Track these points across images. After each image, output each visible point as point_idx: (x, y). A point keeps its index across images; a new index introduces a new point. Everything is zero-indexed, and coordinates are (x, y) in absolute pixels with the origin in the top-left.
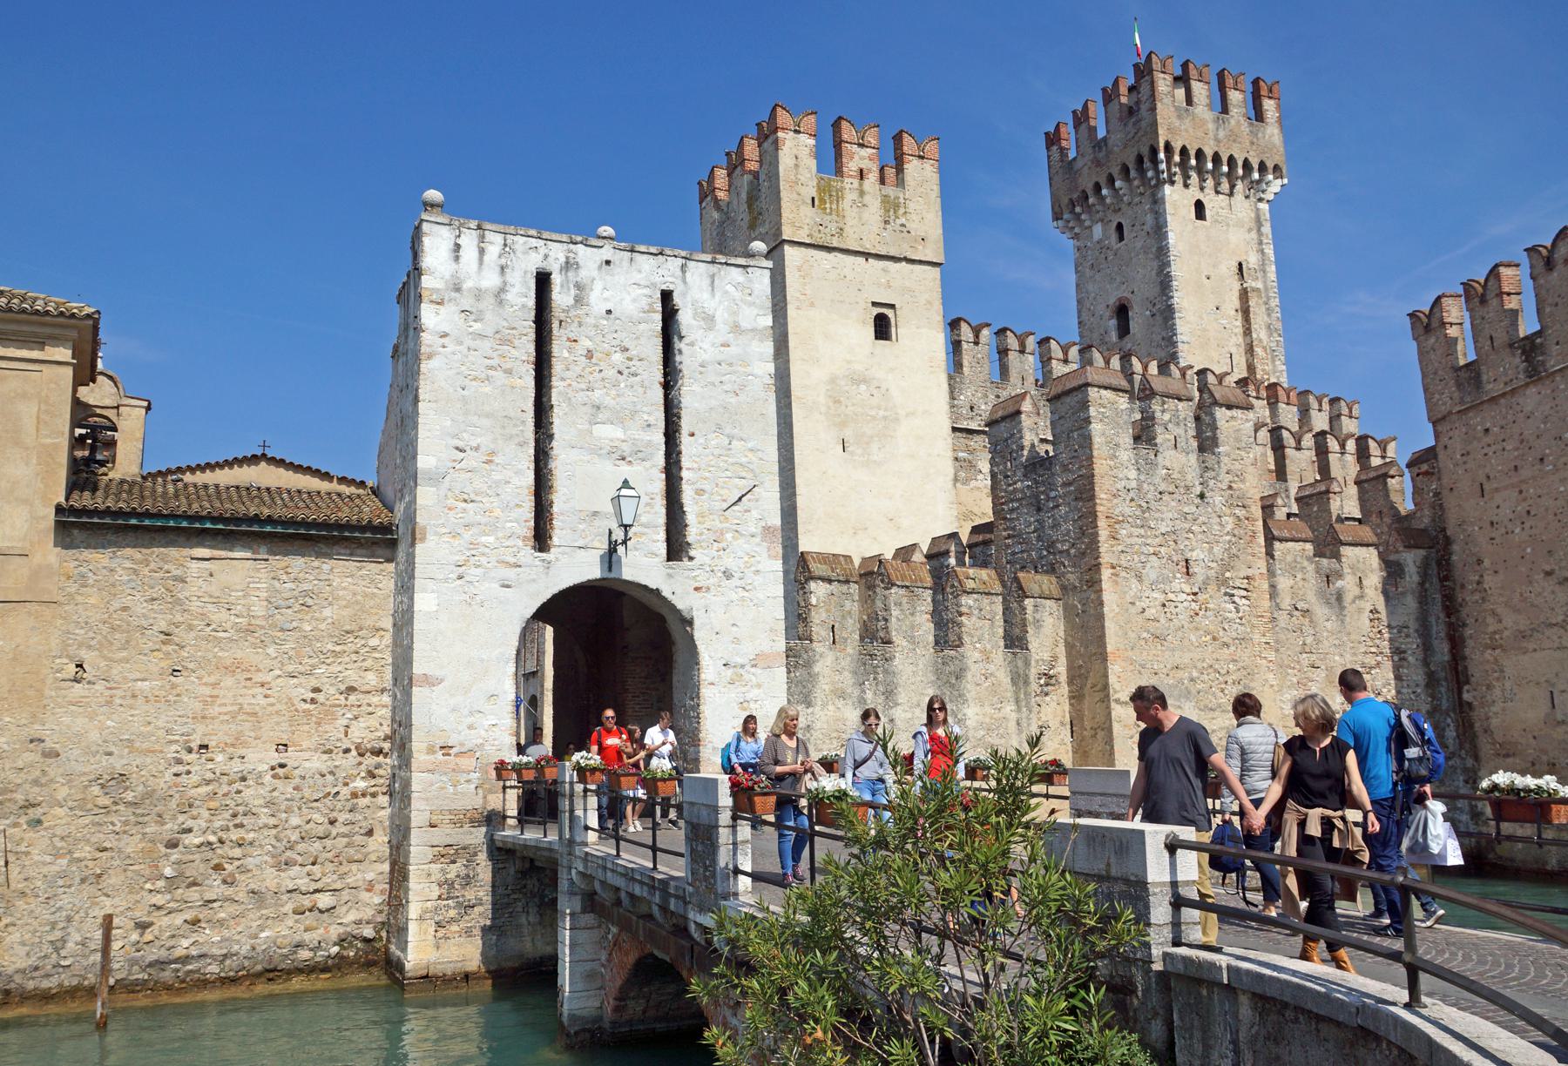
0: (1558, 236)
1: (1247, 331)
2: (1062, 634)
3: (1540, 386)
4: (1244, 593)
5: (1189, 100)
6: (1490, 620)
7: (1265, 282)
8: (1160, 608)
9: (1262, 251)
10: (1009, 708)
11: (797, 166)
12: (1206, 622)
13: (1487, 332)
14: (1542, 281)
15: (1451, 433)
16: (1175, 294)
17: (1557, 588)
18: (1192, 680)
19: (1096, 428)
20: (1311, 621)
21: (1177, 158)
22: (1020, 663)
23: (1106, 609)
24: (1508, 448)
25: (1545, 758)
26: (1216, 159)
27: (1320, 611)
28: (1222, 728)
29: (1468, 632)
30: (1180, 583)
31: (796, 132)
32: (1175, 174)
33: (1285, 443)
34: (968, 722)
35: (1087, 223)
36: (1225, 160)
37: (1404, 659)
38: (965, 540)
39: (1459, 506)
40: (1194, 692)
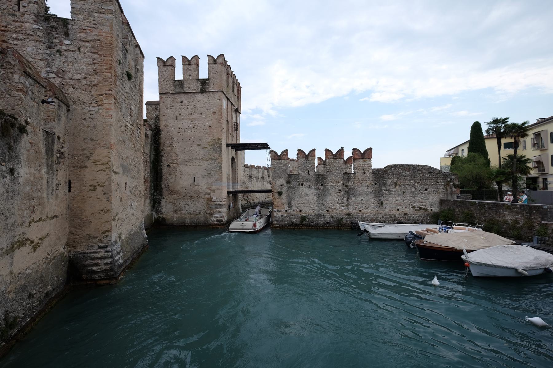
0: (220, 55)
6: (174, 155)
13: (189, 73)
15: (167, 99)
17: (201, 150)
25: (189, 195)
29: (164, 158)
34: (21, 180)
37: (147, 164)
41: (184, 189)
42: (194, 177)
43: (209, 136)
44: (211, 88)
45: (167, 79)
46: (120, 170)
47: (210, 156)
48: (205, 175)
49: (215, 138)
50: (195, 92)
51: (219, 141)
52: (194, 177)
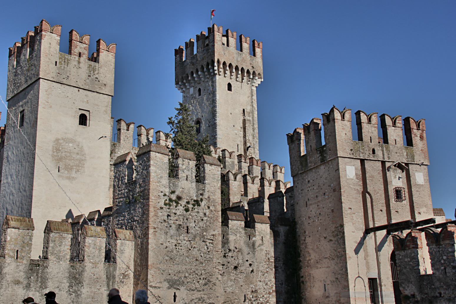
1: (245, 136)
2: (133, 256)
3: (325, 166)
4: (211, 241)
5: (228, 45)
6: (307, 255)
7: (253, 118)
8: (174, 247)
9: (253, 106)
10: (103, 289)
11: (50, 47)
12: (195, 252)
14: (326, 127)
15: (298, 181)
16: (217, 119)
18: (185, 277)
19: (152, 169)
20: (242, 254)
21: (221, 66)
22: (111, 269)
23: (150, 246)
24: (315, 188)
26: (237, 68)
27: (246, 250)
28: (197, 298)
30: (184, 237)
31: (51, 32)
32: (221, 72)
33: (248, 181)
34: (82, 295)
35: (188, 87)
36: (240, 69)
38: (102, 212)
39: (300, 210)
40: (186, 282)
41: (318, 302)
42: (325, 285)
43: (333, 223)
44: (328, 157)
45: (295, 158)
46: (166, 285)
47: (335, 253)
48: (334, 281)
49: (338, 225)
50: (317, 166)
51: (342, 229)
52: (325, 285)
